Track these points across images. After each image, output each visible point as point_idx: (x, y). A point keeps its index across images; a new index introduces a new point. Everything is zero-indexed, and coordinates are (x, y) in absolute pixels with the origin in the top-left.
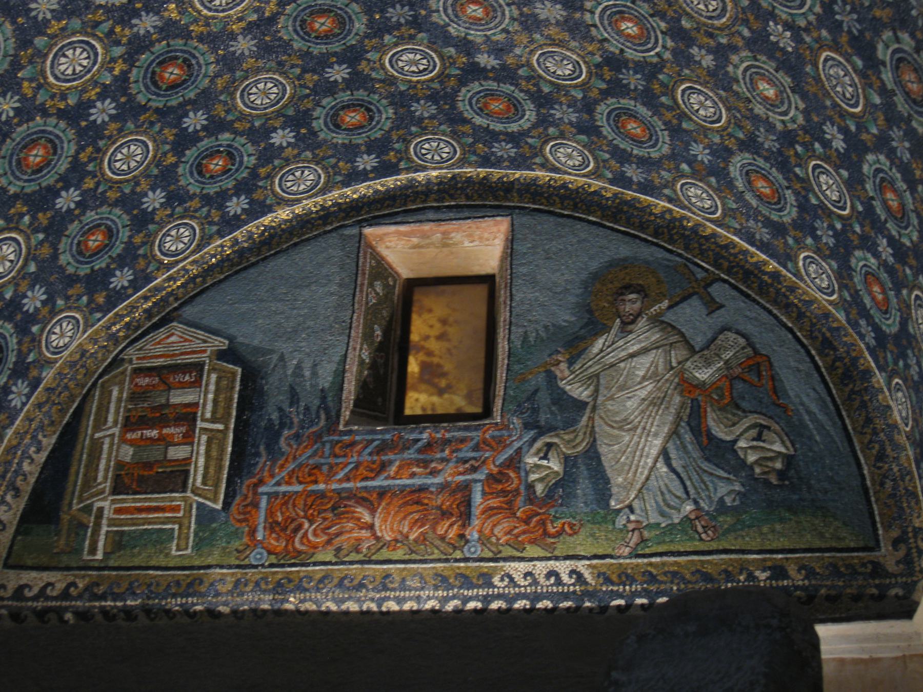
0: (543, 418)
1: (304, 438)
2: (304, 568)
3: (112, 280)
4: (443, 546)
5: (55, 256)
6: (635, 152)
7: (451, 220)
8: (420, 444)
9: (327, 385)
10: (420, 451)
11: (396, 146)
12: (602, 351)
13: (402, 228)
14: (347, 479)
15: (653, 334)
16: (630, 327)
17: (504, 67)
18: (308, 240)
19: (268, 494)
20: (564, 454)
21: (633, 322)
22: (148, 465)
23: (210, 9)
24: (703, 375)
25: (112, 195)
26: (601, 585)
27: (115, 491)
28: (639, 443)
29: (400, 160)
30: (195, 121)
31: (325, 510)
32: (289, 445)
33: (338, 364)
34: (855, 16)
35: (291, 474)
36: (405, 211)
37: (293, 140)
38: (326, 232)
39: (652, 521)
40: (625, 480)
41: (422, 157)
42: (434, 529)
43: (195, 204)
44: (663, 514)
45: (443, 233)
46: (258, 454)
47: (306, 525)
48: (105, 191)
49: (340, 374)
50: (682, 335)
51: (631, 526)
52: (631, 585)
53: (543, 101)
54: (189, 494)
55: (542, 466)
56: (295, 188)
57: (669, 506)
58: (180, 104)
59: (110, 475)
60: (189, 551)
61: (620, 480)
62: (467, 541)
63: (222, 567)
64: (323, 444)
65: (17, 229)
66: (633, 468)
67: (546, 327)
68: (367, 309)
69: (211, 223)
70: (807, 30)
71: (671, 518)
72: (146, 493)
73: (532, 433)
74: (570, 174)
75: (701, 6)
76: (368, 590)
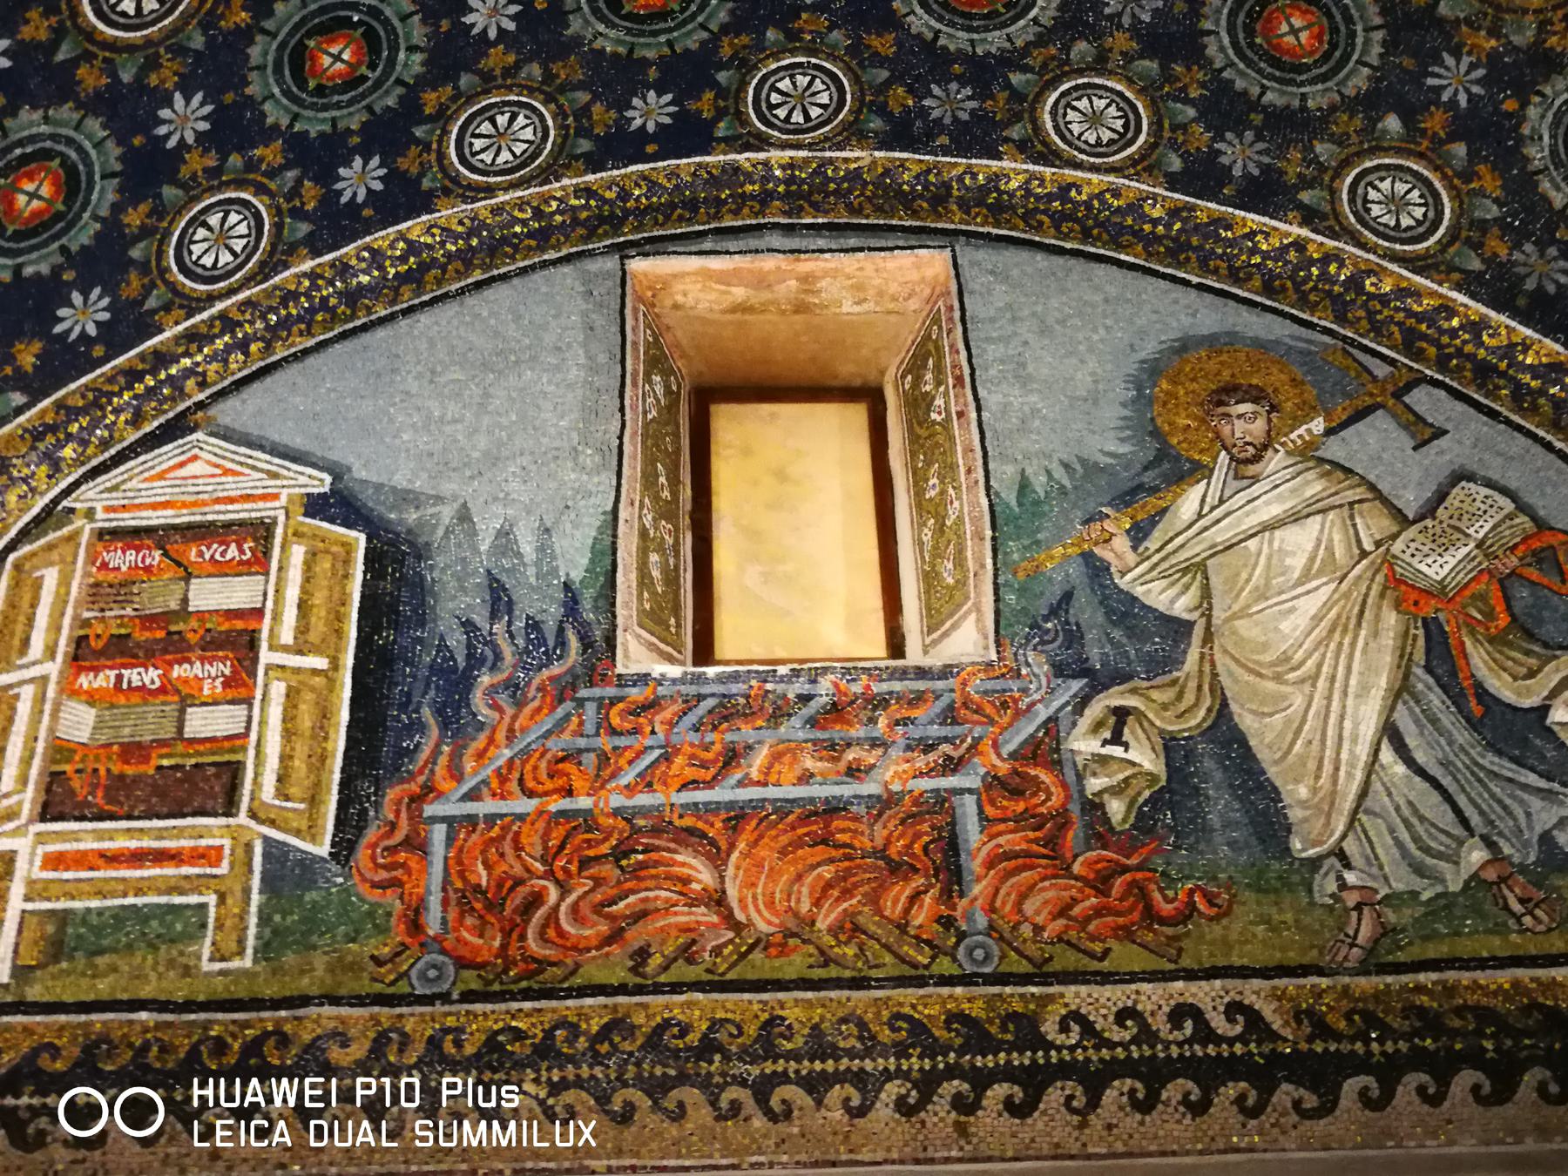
1: (532, 693)
2: (554, 1003)
3: (62, 312)
6: (1269, 97)
7: (822, 251)
8: (814, 705)
9: (577, 575)
10: (813, 722)
11: (722, 77)
12: (1200, 516)
14: (646, 782)
15: (1307, 483)
16: (1252, 469)
18: (504, 278)
19: (449, 820)
20: (1161, 732)
21: (1257, 458)
22: (133, 751)
24: (1438, 568)
25: (90, 78)
26: (1310, 1039)
27: (47, 812)
28: (1328, 707)
29: (720, 114)
31: (597, 859)
32: (495, 707)
33: (600, 530)
36: (719, 232)
37: (511, 26)
38: (545, 265)
39: (1399, 886)
40: (1314, 790)
41: (765, 112)
42: (874, 900)
43: (270, 154)
44: (1419, 870)
45: (806, 279)
46: (420, 727)
47: (553, 894)
48: (73, 63)
50: (1372, 487)
51: (1351, 899)
52: (1382, 1044)
54: (242, 818)
55: (1115, 761)
56: (487, 157)
57: (1427, 850)
59: (34, 772)
60: (247, 962)
61: (1303, 792)
62: (961, 936)
63: (335, 1001)
64: (581, 703)
66: (1328, 767)
67: (1066, 466)
68: (646, 425)
71: (1443, 881)
72: (129, 817)
73: (1076, 685)
74: (1078, 166)
76: (727, 1058)
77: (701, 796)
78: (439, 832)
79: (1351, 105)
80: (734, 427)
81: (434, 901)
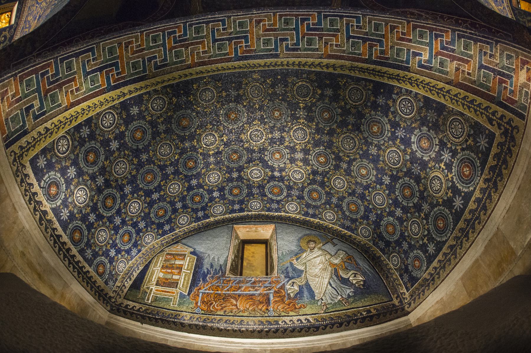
0: (290, 275)
4: (261, 312)
5: (149, 213)
10: (251, 284)
13: (244, 226)
14: (228, 290)
17: (281, 176)
23: (205, 144)
24: (336, 261)
25: (168, 199)
30: (194, 182)
34: (404, 131)
35: (210, 288)
43: (190, 210)
44: (332, 300)
46: (200, 281)
47: (214, 303)
49: (226, 261)
51: (323, 304)
53: (290, 188)
55: (292, 289)
58: (191, 176)
62: (269, 311)
65: (140, 199)
69: (193, 218)
70: (384, 144)
75: (348, 147)
77: (235, 292)
78: (201, 295)
79: (323, 204)
80: (247, 247)
81: (199, 302)
